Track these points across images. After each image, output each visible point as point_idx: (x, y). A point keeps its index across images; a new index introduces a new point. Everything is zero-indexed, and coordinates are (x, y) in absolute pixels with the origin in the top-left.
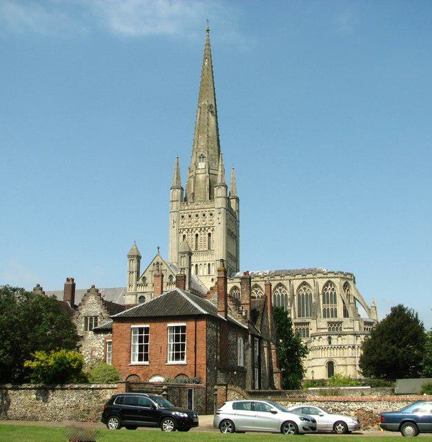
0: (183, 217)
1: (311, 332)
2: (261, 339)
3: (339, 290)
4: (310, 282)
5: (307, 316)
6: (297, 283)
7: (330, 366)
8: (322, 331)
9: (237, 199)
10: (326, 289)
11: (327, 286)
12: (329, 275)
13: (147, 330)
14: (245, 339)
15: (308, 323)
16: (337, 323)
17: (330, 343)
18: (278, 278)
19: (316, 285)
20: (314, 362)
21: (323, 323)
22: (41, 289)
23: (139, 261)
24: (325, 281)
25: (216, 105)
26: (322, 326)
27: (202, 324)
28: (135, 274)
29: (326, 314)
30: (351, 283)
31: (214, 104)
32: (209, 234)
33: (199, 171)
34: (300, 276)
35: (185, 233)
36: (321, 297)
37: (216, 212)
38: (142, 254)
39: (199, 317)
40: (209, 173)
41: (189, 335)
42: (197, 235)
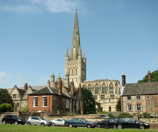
0: (69, 64)
1: (105, 98)
2: (76, 100)
3: (114, 85)
4: (106, 83)
5: (105, 93)
6: (102, 84)
7: (110, 108)
8: (108, 98)
9: (85, 59)
10: (110, 85)
11: (111, 84)
12: (111, 81)
13: (37, 98)
14: (70, 100)
15: (104, 95)
16: (113, 95)
17: (110, 101)
18: (96, 82)
19: (107, 84)
20: (105, 107)
21: (109, 95)
22: (16, 86)
23: (54, 78)
24: (110, 83)
25: (79, 32)
26: (109, 96)
27: (51, 96)
28: (53, 82)
29: (110, 92)
30: (118, 83)
31: (78, 31)
32: (76, 70)
33: (74, 51)
34: (103, 82)
35: (69, 69)
36: (109, 87)
37: (78, 63)
38: (55, 76)
39: (51, 94)
40: (77, 52)
41: (48, 99)
42: (73, 70)
